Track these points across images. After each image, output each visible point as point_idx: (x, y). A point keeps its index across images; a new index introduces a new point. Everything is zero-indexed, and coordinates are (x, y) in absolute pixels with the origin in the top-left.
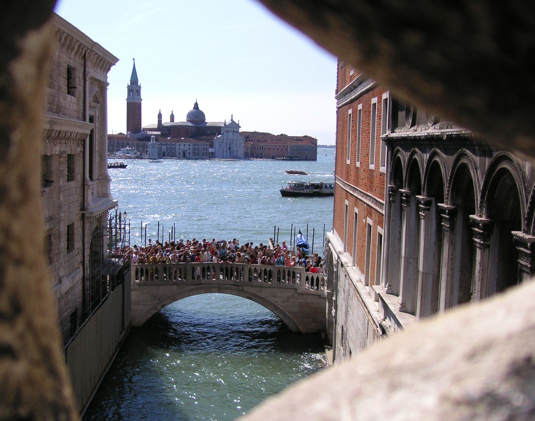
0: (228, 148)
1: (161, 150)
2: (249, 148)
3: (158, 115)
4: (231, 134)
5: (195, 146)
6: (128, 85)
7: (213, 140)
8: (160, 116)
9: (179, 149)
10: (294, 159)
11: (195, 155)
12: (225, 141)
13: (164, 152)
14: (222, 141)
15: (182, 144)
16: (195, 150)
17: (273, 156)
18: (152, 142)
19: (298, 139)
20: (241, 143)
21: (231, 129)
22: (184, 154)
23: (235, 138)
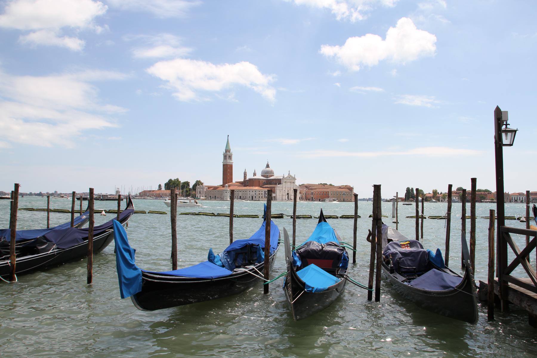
0: (287, 194)
1: (239, 195)
2: (304, 194)
3: (244, 172)
4: (289, 184)
5: (259, 191)
6: (224, 153)
7: (275, 188)
9: (250, 194)
11: (259, 198)
12: (284, 189)
14: (282, 188)
16: (259, 194)
17: (320, 199)
19: (340, 188)
21: (288, 181)
22: (252, 197)
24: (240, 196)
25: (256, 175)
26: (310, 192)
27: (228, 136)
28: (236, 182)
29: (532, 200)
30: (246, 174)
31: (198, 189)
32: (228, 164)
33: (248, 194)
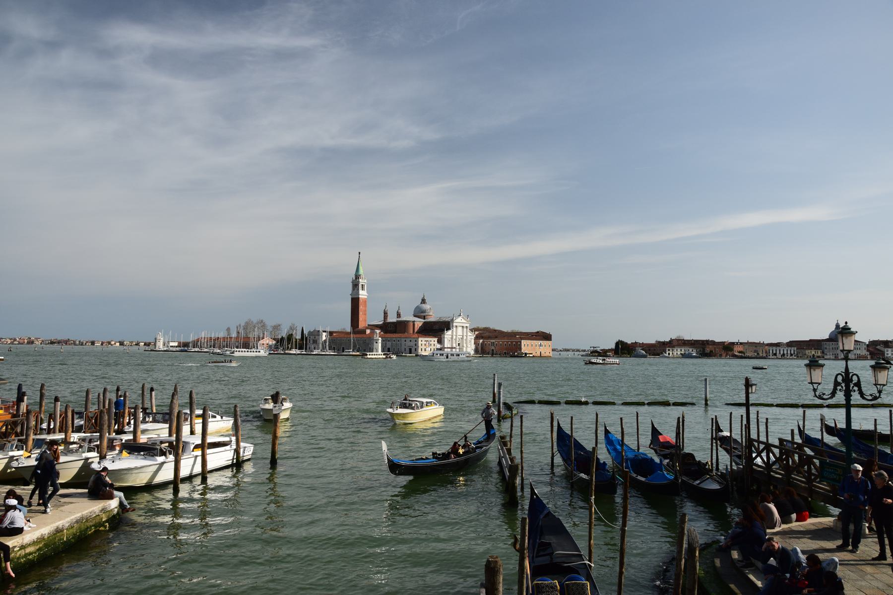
1: (386, 346)
2: (480, 345)
5: (422, 341)
6: (353, 280)
7: (441, 335)
8: (385, 314)
10: (528, 355)
11: (422, 350)
13: (389, 349)
15: (408, 340)
17: (505, 352)
18: (375, 336)
20: (471, 339)
23: (465, 334)
24: (388, 347)
25: (400, 314)
26: (489, 341)
27: (359, 253)
28: (369, 325)
29: (797, 354)
30: (387, 313)
31: (311, 337)
32: (360, 296)
33: (403, 345)
